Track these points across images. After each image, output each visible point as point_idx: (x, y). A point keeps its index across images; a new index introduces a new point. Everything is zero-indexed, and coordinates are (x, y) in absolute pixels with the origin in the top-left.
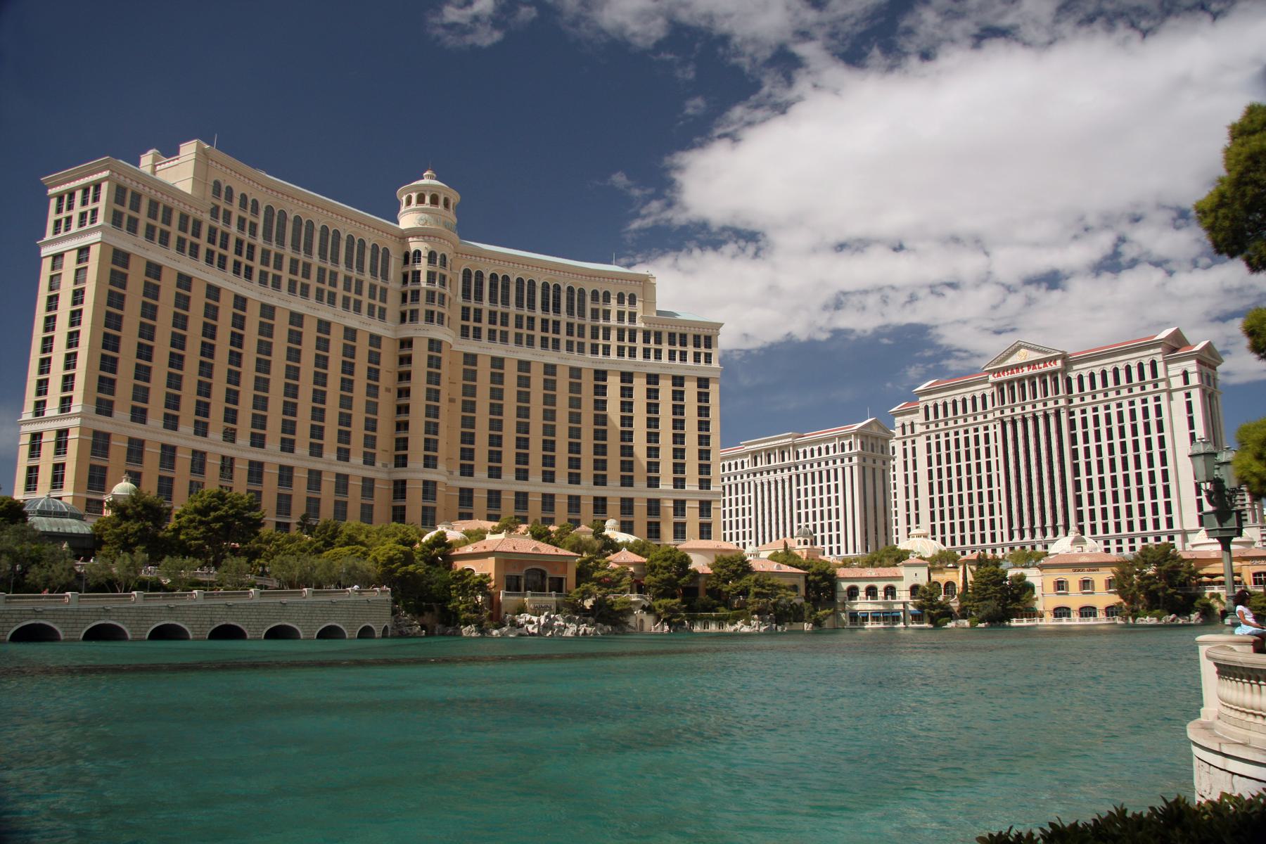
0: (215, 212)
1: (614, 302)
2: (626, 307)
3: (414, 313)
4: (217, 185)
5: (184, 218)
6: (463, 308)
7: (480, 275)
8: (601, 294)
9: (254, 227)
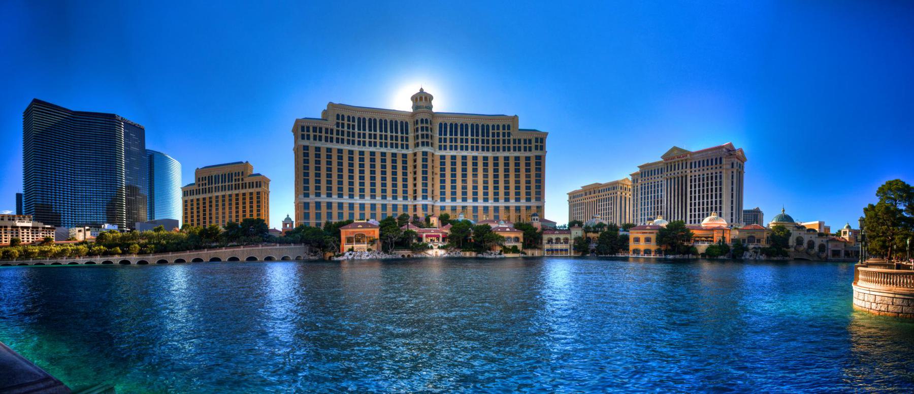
2: (506, 131)
4: (338, 116)
9: (354, 126)
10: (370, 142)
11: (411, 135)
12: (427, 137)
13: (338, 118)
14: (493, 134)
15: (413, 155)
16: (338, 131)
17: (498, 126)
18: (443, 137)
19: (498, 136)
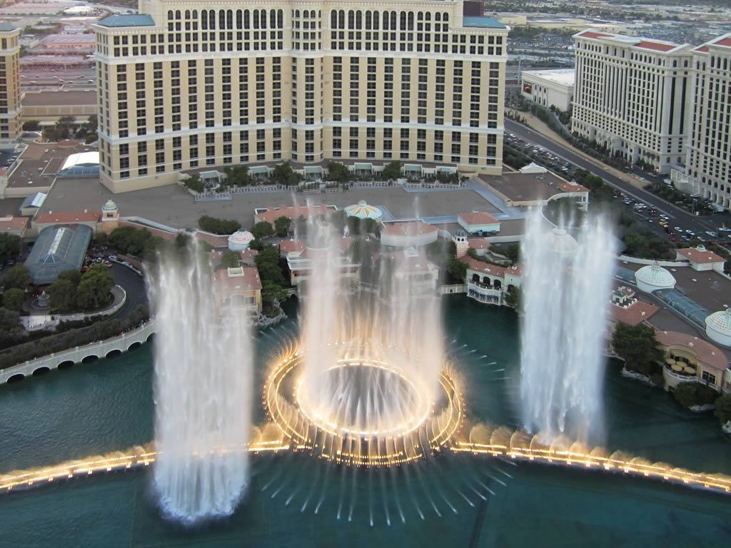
0: (170, 27)
1: (433, 17)
2: (442, 22)
3: (298, 45)
4: (170, 13)
5: (153, 37)
6: (332, 32)
11: (287, 28)
12: (313, 35)
13: (170, 17)
15: (291, 60)
16: (171, 36)
17: (428, 14)
18: (338, 30)
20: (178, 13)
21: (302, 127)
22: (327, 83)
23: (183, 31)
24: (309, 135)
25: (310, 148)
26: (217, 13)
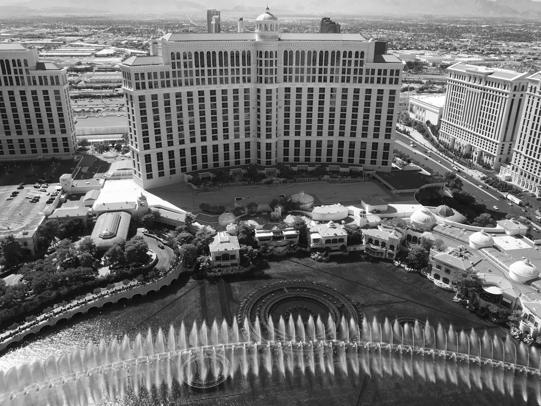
2: (359, 59)
5: (162, 74)
7: (291, 52)
8: (348, 53)
9: (191, 63)
10: (210, 80)
11: (253, 67)
14: (344, 61)
16: (174, 73)
17: (350, 53)
19: (350, 64)
20: (178, 54)
21: (264, 141)
22: (280, 107)
23: (183, 68)
24: (269, 146)
25: (269, 156)
26: (205, 53)
